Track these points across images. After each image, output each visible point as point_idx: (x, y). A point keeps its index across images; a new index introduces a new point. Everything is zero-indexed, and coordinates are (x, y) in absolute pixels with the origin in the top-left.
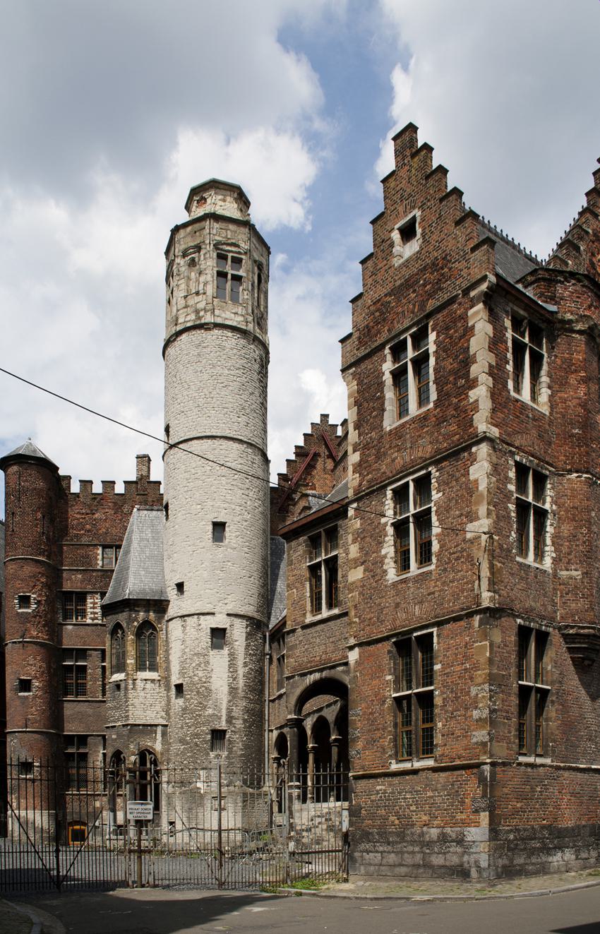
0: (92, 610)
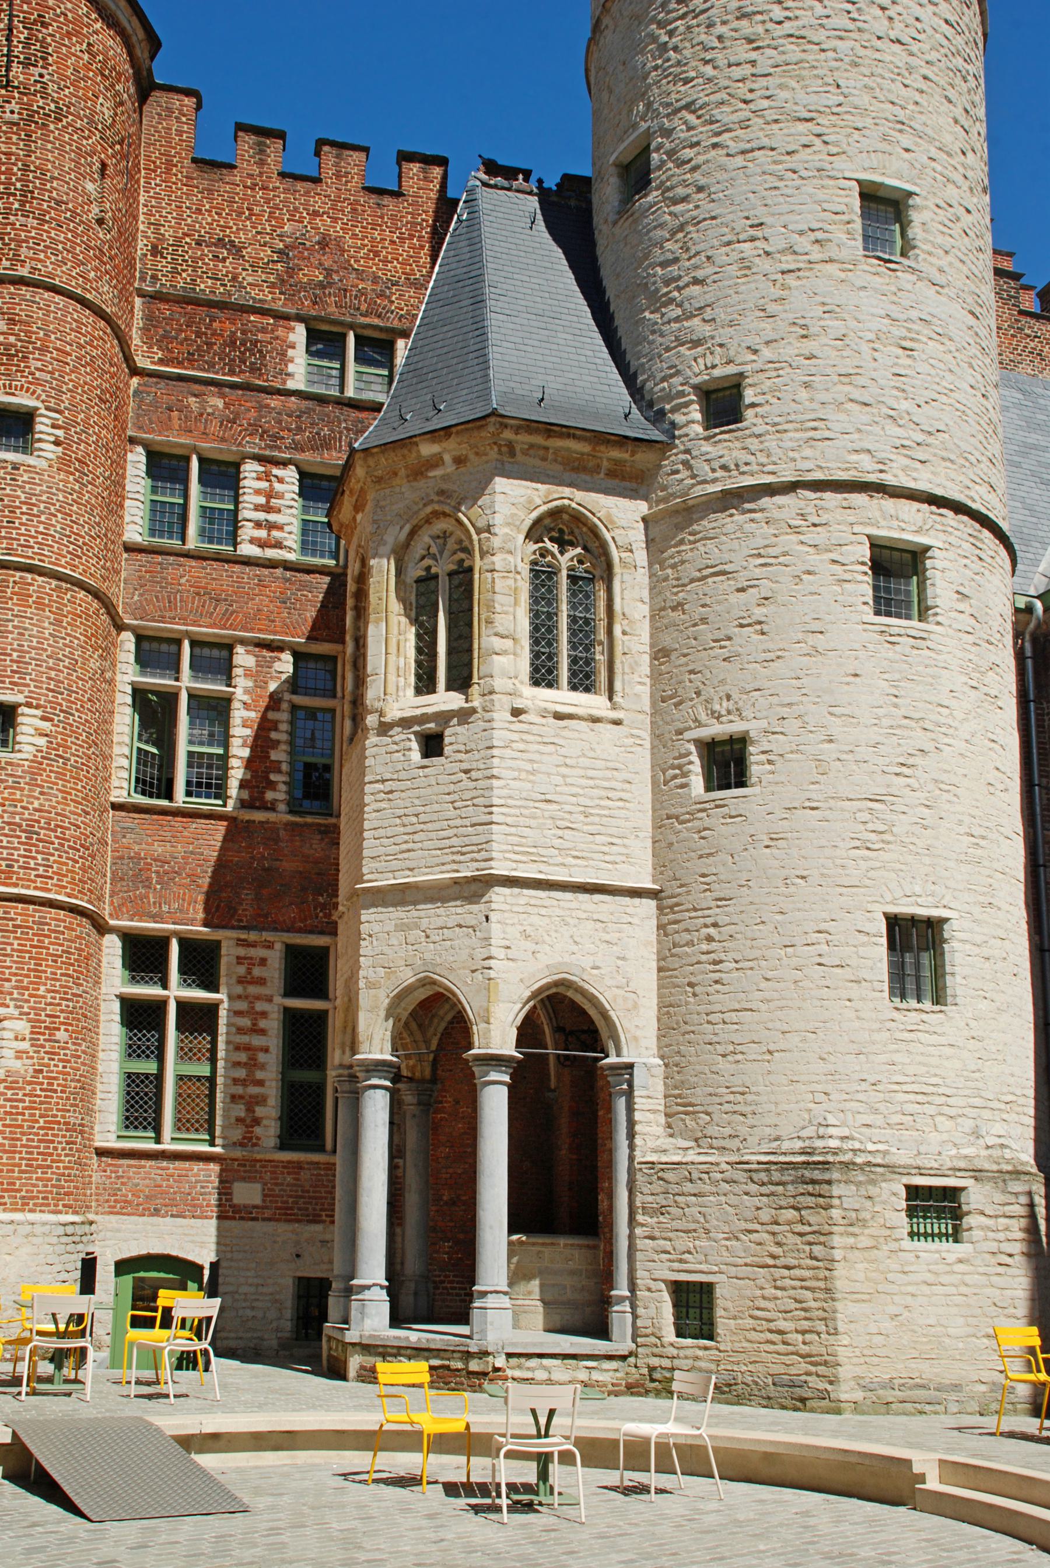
0: (261, 516)
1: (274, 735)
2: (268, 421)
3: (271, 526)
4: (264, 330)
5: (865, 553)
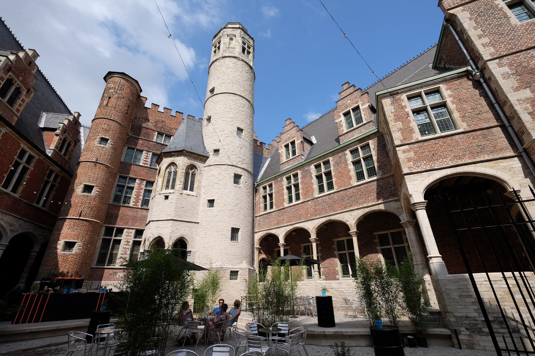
0: (145, 159)
1: (141, 194)
2: (149, 146)
3: (147, 161)
4: (151, 132)
5: (233, 175)
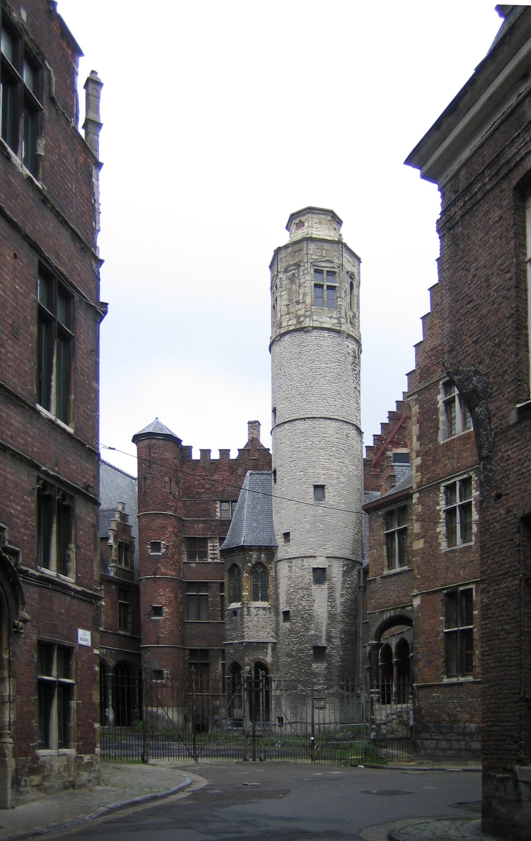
0: (212, 552)
